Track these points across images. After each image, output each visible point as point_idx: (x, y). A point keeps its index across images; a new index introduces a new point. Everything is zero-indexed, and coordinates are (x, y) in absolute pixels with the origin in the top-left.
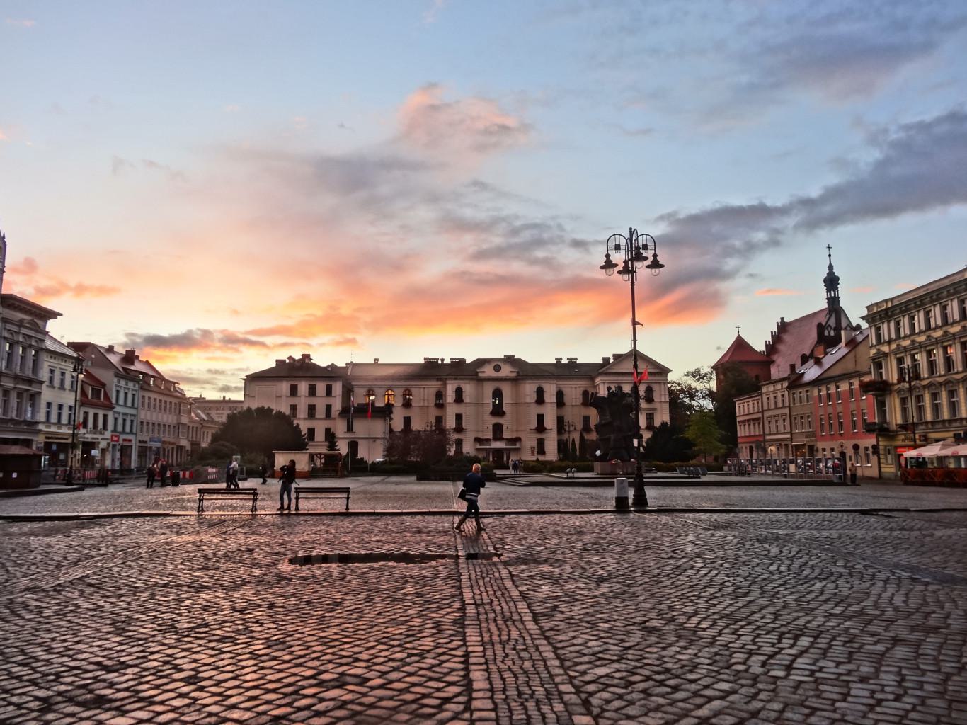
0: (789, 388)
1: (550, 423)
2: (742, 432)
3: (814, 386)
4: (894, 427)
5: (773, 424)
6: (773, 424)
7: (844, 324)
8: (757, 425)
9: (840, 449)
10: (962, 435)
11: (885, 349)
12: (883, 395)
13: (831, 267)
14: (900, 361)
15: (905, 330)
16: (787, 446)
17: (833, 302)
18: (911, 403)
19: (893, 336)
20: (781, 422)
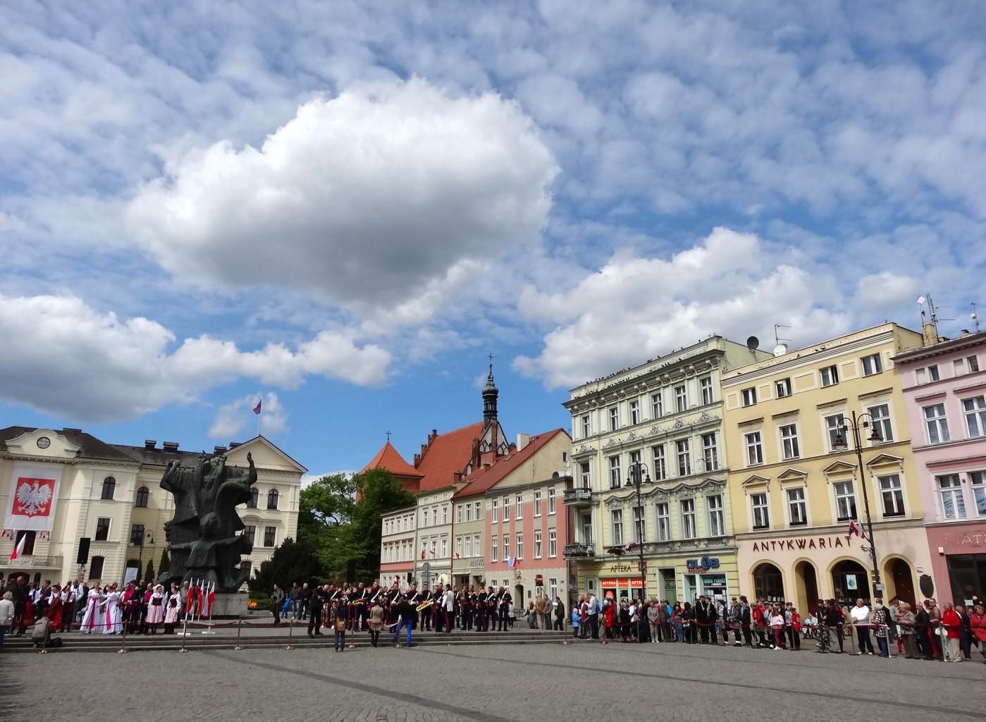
0: (454, 500)
1: (119, 532)
2: (387, 556)
3: (487, 497)
4: (600, 551)
5: (430, 547)
6: (430, 547)
7: (500, 439)
8: (408, 547)
10: (699, 564)
11: (595, 444)
12: (589, 507)
14: (614, 460)
15: (624, 416)
17: (491, 413)
18: (628, 516)
19: (605, 426)
20: (439, 541)
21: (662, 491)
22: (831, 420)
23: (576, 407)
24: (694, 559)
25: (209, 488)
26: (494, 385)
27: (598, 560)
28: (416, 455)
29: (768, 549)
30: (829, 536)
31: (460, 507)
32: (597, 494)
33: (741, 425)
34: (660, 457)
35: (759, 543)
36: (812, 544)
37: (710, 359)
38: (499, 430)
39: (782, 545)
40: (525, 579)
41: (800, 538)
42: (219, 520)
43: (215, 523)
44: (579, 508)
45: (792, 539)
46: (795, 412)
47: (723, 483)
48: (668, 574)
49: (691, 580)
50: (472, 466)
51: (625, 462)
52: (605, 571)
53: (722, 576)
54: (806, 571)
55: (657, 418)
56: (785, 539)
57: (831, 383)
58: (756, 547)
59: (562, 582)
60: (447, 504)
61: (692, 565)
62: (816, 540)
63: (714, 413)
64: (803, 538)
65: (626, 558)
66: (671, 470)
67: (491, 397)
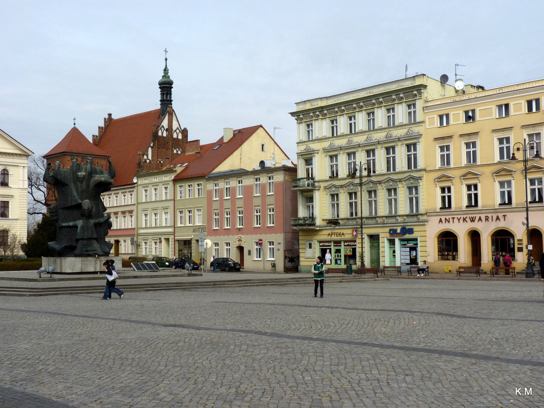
0: (175, 181)
4: (318, 222)
7: (175, 125)
9: (237, 244)
10: (399, 231)
11: (315, 146)
12: (312, 191)
13: (166, 70)
16: (167, 240)
18: (344, 199)
21: (372, 182)
22: (501, 141)
23: (301, 116)
24: (395, 228)
25: (82, 182)
26: (169, 77)
27: (318, 228)
28: (93, 136)
29: (449, 222)
30: (492, 215)
31: (180, 186)
32: (318, 182)
33: (436, 139)
34: (372, 158)
35: (443, 218)
36: (480, 219)
37: (417, 90)
38: (174, 118)
39: (459, 220)
40: (245, 242)
41: (472, 216)
42: (94, 205)
43: (92, 207)
44: (302, 191)
45: (461, 216)
46: (477, 133)
47: (420, 178)
48: (374, 238)
49: (392, 242)
50: (152, 147)
51: (343, 162)
52: (324, 236)
53: (416, 240)
54: (475, 236)
55: (372, 129)
56: (462, 216)
57: (504, 116)
58: (441, 221)
59: (279, 244)
60: (168, 184)
61: (393, 232)
62: (483, 217)
63: (416, 129)
64: (474, 216)
65: (341, 227)
66: (381, 167)
67: (166, 87)
